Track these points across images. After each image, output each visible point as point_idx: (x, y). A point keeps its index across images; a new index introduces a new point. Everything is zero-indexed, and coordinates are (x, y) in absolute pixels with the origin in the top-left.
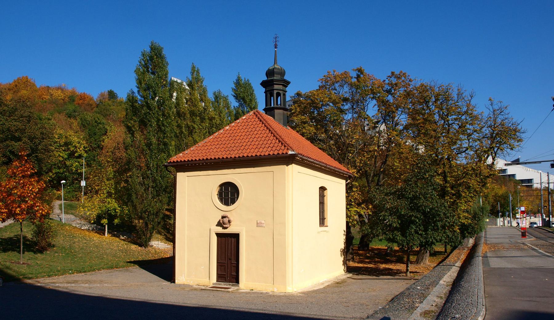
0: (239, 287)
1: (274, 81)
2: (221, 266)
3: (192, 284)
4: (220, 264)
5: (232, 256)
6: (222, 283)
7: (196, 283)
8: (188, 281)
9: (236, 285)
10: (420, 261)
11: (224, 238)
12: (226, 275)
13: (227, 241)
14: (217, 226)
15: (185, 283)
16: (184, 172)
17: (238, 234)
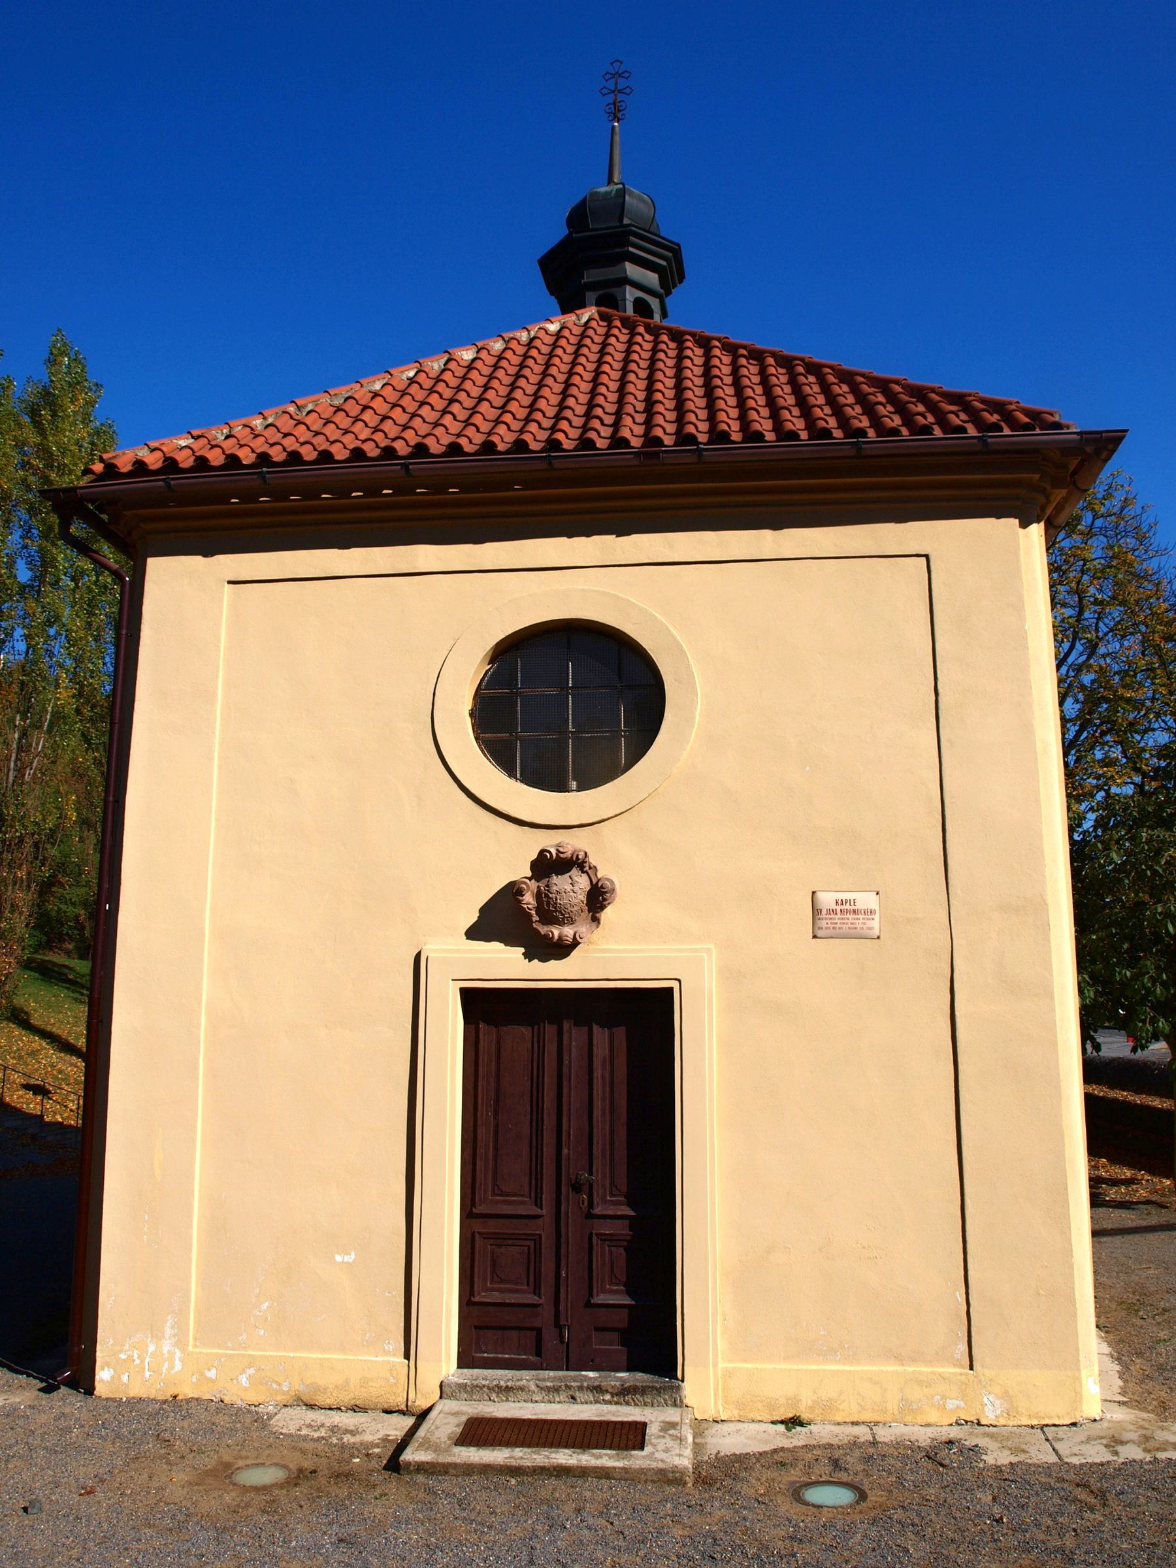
0: (678, 1403)
2: (499, 1239)
3: (252, 1397)
4: (492, 1226)
5: (597, 1163)
6: (526, 1377)
7: (289, 1386)
8: (212, 1374)
9: (659, 1391)
11: (526, 1031)
12: (547, 1314)
13: (551, 1048)
14: (474, 933)
15: (187, 1391)
17: (671, 990)
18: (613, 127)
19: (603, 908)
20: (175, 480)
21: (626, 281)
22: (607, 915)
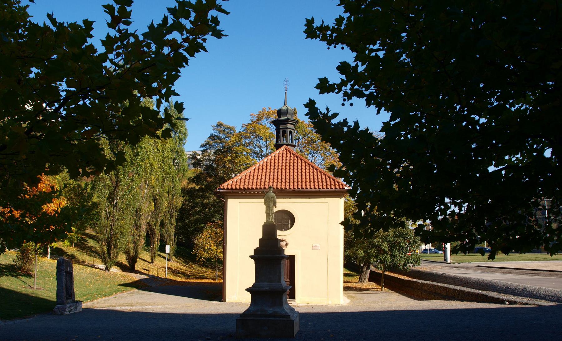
1: (289, 121)
9: (294, 301)
10: (363, 280)
15: (237, 302)
16: (236, 199)
18: (285, 93)
19: (287, 246)
20: (233, 190)
21: (288, 128)
22: (287, 247)
